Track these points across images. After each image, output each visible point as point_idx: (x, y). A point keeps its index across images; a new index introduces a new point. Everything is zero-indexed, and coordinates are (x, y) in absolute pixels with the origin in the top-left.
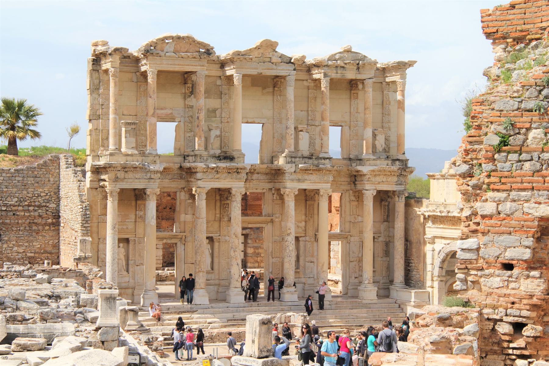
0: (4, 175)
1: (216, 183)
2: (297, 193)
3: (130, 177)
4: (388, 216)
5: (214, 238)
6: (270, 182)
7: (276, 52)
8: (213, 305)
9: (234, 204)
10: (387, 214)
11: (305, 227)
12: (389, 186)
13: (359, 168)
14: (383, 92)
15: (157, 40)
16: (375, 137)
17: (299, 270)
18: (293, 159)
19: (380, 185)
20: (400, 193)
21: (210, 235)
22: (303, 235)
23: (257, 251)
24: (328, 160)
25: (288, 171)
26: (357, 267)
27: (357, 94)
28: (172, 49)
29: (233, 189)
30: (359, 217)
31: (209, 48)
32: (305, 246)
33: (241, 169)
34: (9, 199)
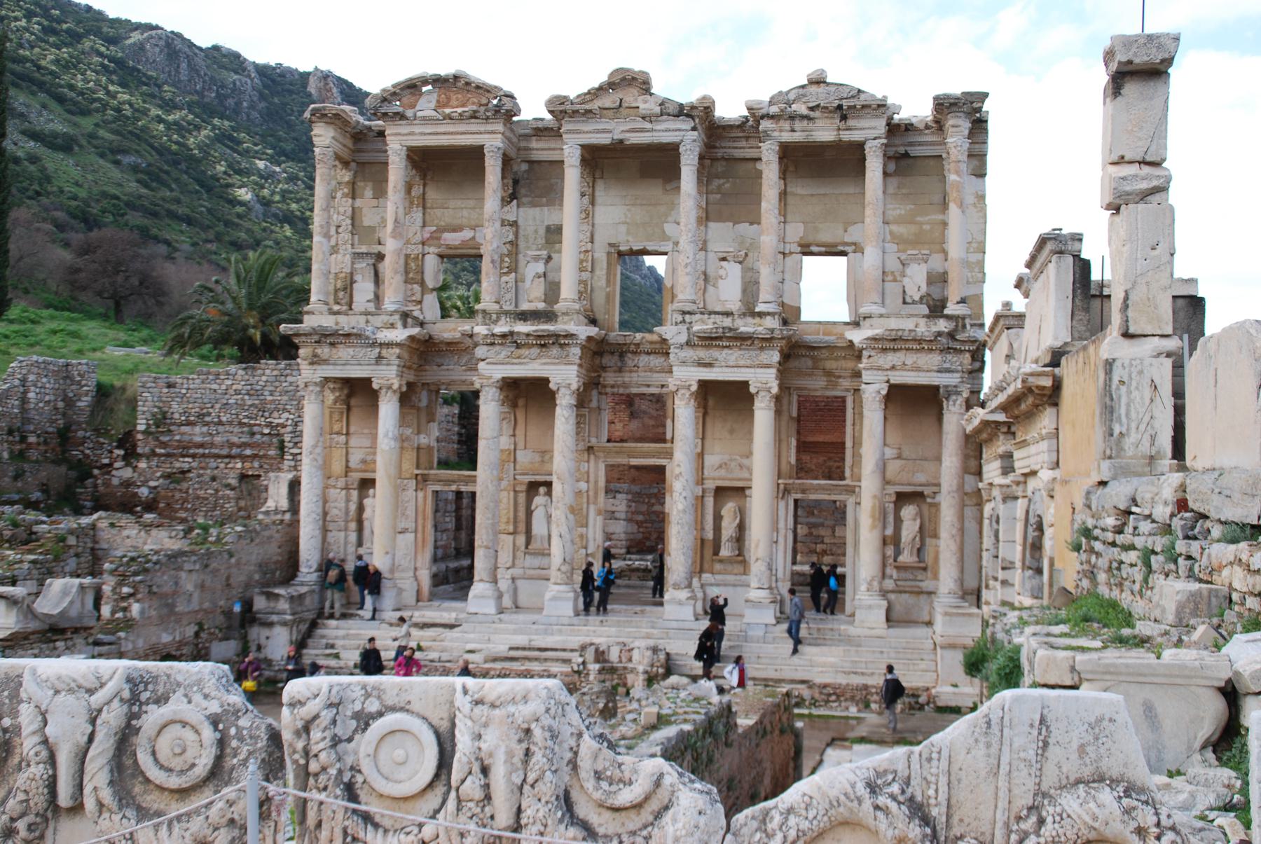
0: (268, 372)
2: (694, 388)
3: (340, 354)
7: (651, 94)
8: (502, 616)
9: (558, 410)
15: (394, 86)
17: (740, 558)
18: (687, 317)
19: (897, 373)
20: (952, 392)
23: (815, 532)
24: (768, 318)
28: (433, 105)
33: (566, 336)
34: (276, 414)
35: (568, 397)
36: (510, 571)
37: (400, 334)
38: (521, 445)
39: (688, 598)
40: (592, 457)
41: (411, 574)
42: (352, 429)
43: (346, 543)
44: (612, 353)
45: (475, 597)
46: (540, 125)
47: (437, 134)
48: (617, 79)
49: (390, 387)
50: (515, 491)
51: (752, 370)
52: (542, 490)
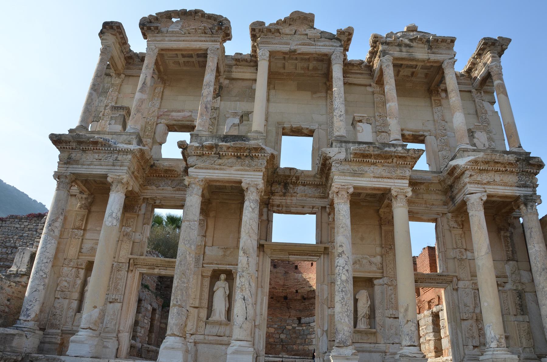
1: (217, 171)
2: (351, 190)
3: (88, 157)
4: (514, 252)
5: (233, 271)
6: (323, 198)
7: (314, 29)
9: (246, 204)
10: (511, 249)
11: (382, 264)
12: (506, 188)
13: (453, 163)
14: (474, 101)
15: (156, 14)
16: (472, 135)
17: (374, 330)
18: (343, 144)
19: (491, 187)
21: (228, 267)
22: (379, 275)
25: (334, 158)
26: (475, 329)
27: (440, 100)
29: (243, 181)
30: (468, 252)
31: (221, 19)
32: (382, 293)
35: (255, 194)
36: (194, 336)
37: (134, 147)
38: (209, 243)
39: (353, 354)
40: (262, 253)
41: (115, 335)
42: (89, 227)
43: (69, 308)
44: (280, 184)
45: (166, 348)
46: (239, 57)
47: (181, 41)
48: (295, 16)
49: (120, 182)
50: (202, 276)
51: (392, 181)
52: (223, 276)
